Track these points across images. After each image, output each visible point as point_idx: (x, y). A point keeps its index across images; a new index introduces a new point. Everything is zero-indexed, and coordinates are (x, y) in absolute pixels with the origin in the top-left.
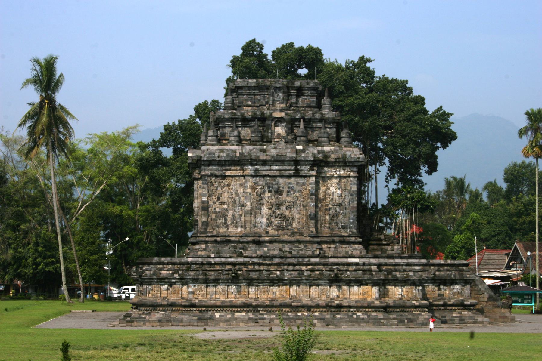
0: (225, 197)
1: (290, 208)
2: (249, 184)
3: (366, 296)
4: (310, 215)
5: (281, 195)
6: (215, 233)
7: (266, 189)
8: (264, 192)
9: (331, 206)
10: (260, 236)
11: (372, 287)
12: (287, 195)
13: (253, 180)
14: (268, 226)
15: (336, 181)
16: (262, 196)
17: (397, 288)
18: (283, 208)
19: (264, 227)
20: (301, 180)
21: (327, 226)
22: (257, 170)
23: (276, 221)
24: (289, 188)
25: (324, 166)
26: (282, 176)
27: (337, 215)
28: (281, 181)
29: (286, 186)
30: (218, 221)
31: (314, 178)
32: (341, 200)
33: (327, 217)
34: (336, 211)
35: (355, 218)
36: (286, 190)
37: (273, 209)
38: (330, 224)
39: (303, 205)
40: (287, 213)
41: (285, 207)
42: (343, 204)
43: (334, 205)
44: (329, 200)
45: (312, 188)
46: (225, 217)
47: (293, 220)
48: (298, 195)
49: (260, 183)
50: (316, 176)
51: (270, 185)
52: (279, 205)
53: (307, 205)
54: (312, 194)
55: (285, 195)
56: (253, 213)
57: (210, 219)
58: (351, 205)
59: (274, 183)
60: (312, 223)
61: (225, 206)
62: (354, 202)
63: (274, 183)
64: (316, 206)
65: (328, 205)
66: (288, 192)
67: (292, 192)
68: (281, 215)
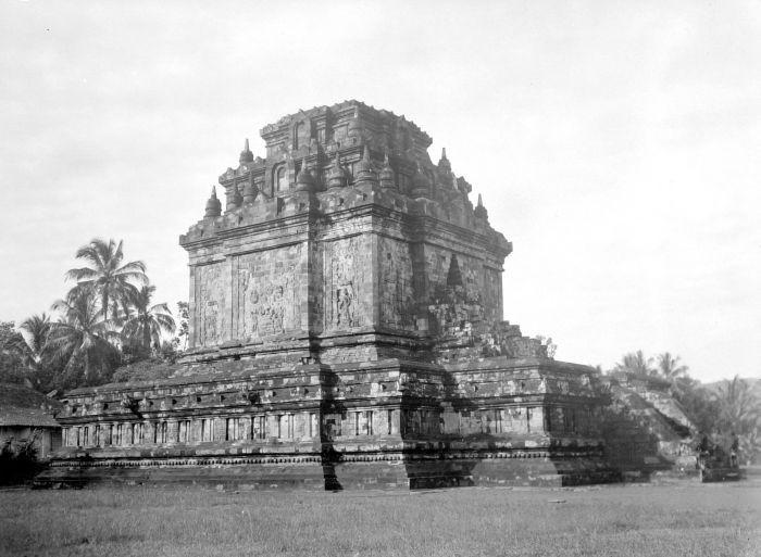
0: (215, 297)
2: (229, 269)
6: (201, 348)
9: (339, 288)
10: (240, 346)
15: (343, 243)
20: (293, 250)
21: (336, 320)
27: (348, 301)
30: (208, 331)
31: (306, 243)
34: (347, 294)
36: (273, 269)
38: (339, 315)
40: (275, 306)
46: (213, 322)
57: (198, 331)
61: (215, 308)
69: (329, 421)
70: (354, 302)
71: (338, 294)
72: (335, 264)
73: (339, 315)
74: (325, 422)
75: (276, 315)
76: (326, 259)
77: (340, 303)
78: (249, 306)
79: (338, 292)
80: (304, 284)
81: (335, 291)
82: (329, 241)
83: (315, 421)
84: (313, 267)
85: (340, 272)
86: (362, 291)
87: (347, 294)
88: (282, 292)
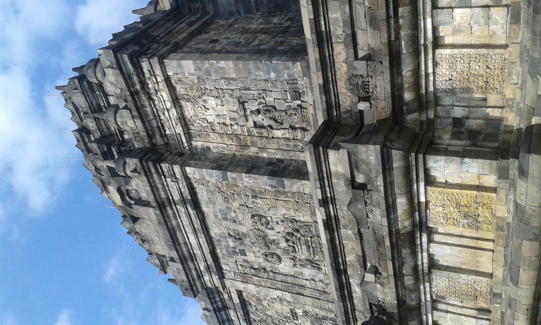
1: (268, 223)
3: (484, 214)
4: (273, 187)
5: (245, 235)
7: (240, 258)
8: (246, 261)
9: (251, 124)
11: (430, 181)
12: (241, 224)
13: (228, 275)
14: (319, 269)
16: (256, 267)
17: (443, 31)
18: (271, 235)
19: (321, 276)
22: (208, 268)
23: (303, 254)
24: (226, 219)
25: (164, 136)
26: (206, 229)
27: (269, 109)
28: (214, 231)
29: (224, 223)
32: (227, 97)
33: (278, 133)
34: (258, 112)
35: (263, 64)
36: (232, 226)
37: (278, 252)
38: (293, 128)
39: (255, 197)
40: (280, 228)
41: (270, 232)
42: (237, 93)
43: (246, 116)
44: (236, 127)
45: (211, 176)
47: (293, 221)
48: (236, 205)
49: (232, 265)
50: (183, 166)
51: (230, 250)
52: (267, 242)
53: (253, 190)
54: (225, 178)
55: (243, 229)
56: (297, 289)
58: (234, 76)
59: (224, 243)
60: (291, 186)
62: (223, 69)
63: (224, 243)
64: (252, 166)
65: (249, 131)
66: (235, 222)
67: (233, 215)
68: (287, 241)
69: (456, 135)
70: (270, 100)
71: (262, 127)
72: (218, 128)
73: (293, 128)
74: (457, 144)
75: (296, 232)
76: (218, 145)
77: (272, 123)
78: (285, 266)
79: (256, 125)
80: (247, 180)
81: (255, 131)
82: (189, 136)
83: (442, 168)
84: (222, 164)
85: (228, 122)
86: (248, 84)
87: (258, 112)
88: (260, 217)
